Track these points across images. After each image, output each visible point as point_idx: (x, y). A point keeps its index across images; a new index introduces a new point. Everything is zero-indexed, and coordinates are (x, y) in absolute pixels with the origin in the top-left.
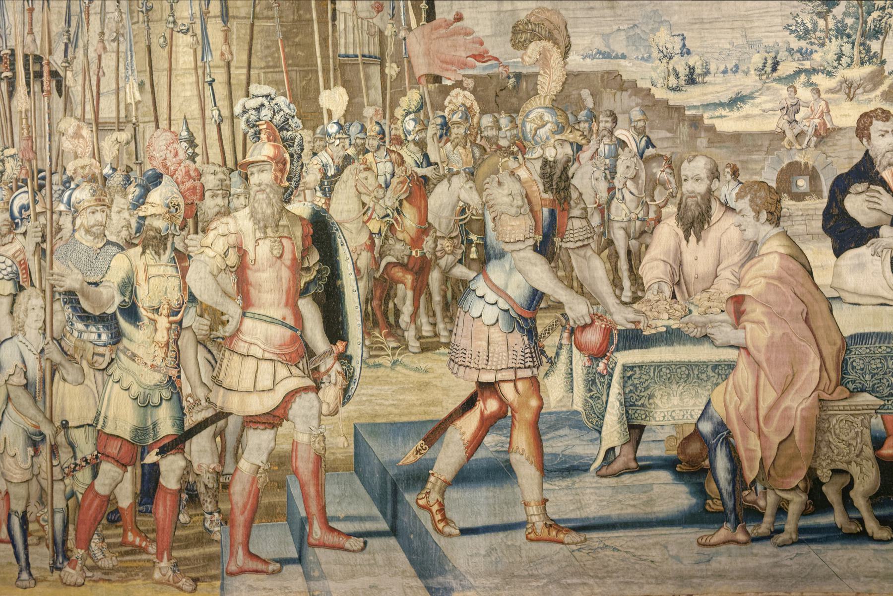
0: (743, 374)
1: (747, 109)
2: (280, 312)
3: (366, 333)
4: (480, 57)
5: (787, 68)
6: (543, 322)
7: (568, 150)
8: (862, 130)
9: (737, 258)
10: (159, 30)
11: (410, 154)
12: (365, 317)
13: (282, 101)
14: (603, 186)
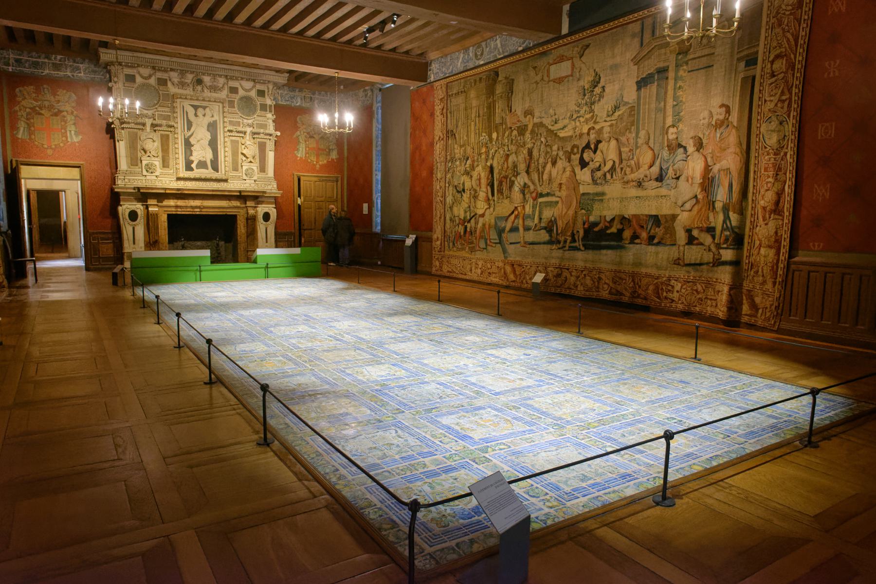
0: (560, 204)
1: (566, 129)
2: (484, 190)
3: (497, 194)
4: (518, 121)
5: (574, 117)
6: (526, 191)
7: (532, 145)
8: (588, 134)
9: (561, 172)
10: (469, 121)
11: (506, 148)
12: (497, 190)
13: (487, 137)
14: (538, 154)
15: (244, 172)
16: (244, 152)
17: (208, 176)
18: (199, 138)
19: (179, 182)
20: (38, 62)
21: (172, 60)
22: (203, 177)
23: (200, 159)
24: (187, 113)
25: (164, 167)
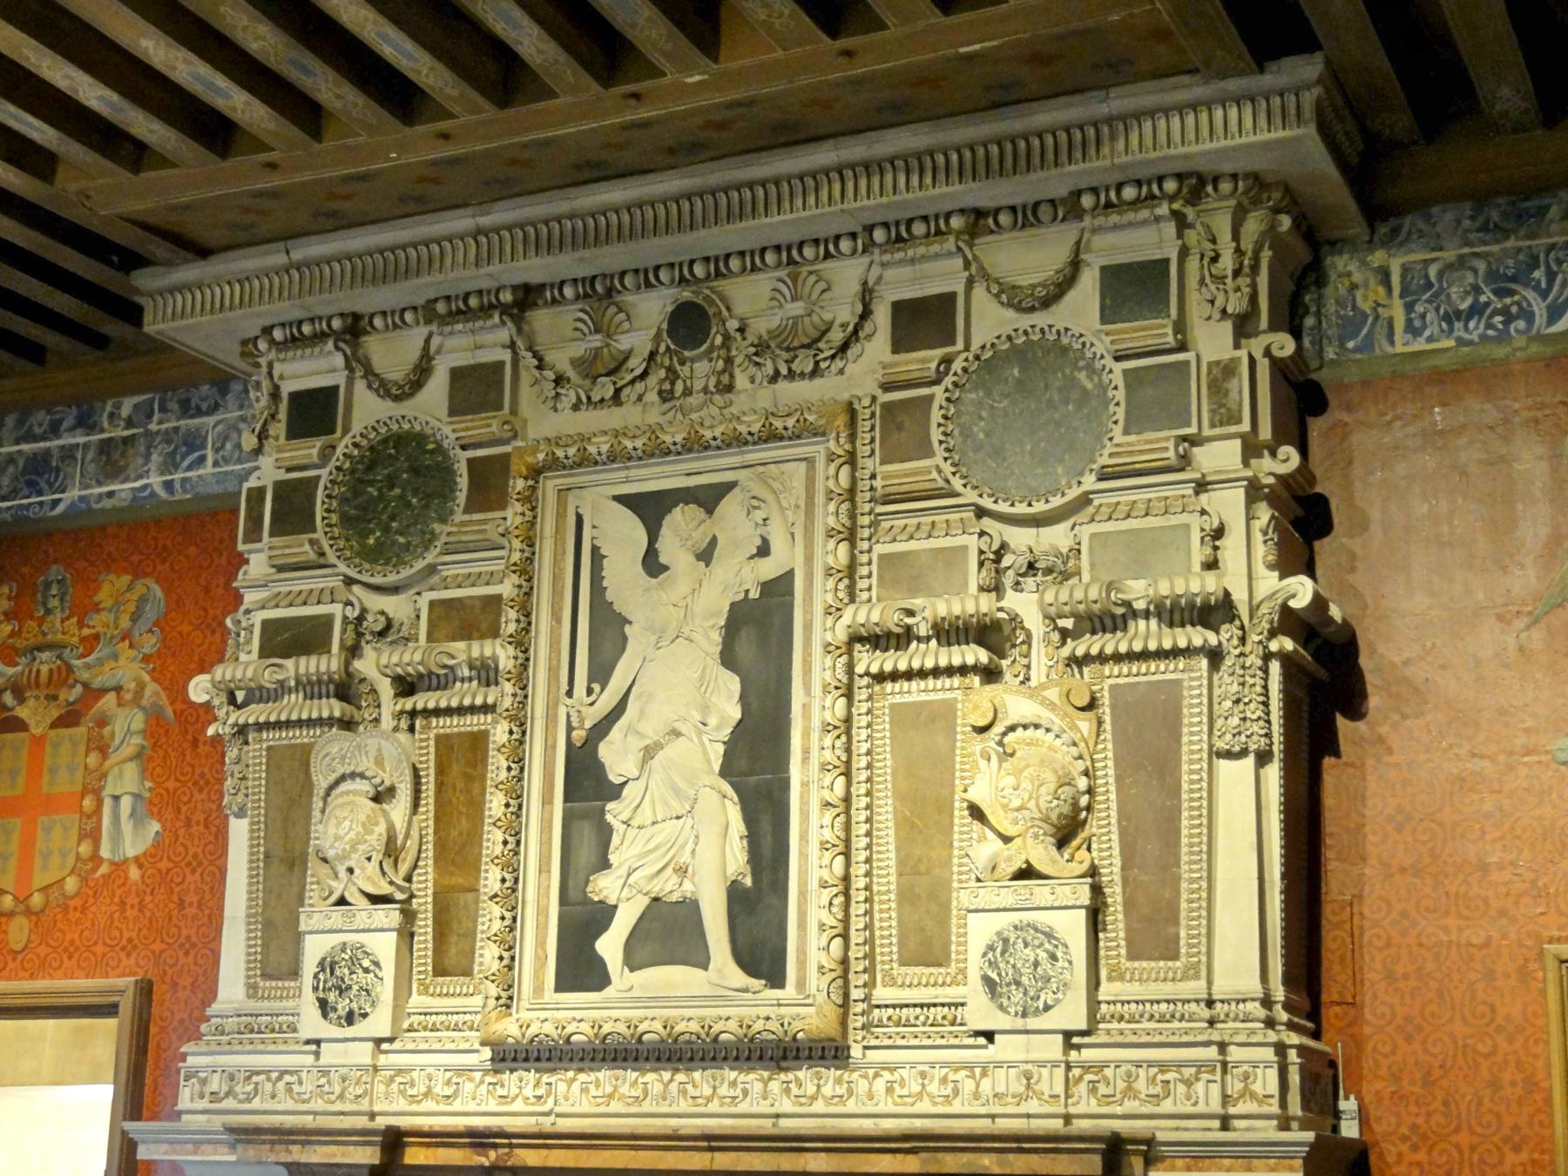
15: (975, 966)
16: (978, 794)
17: (688, 1024)
18: (652, 729)
19: (511, 1080)
20: (47, 453)
21: (485, 221)
22: (653, 1029)
23: (658, 887)
24: (597, 557)
25: (440, 971)
